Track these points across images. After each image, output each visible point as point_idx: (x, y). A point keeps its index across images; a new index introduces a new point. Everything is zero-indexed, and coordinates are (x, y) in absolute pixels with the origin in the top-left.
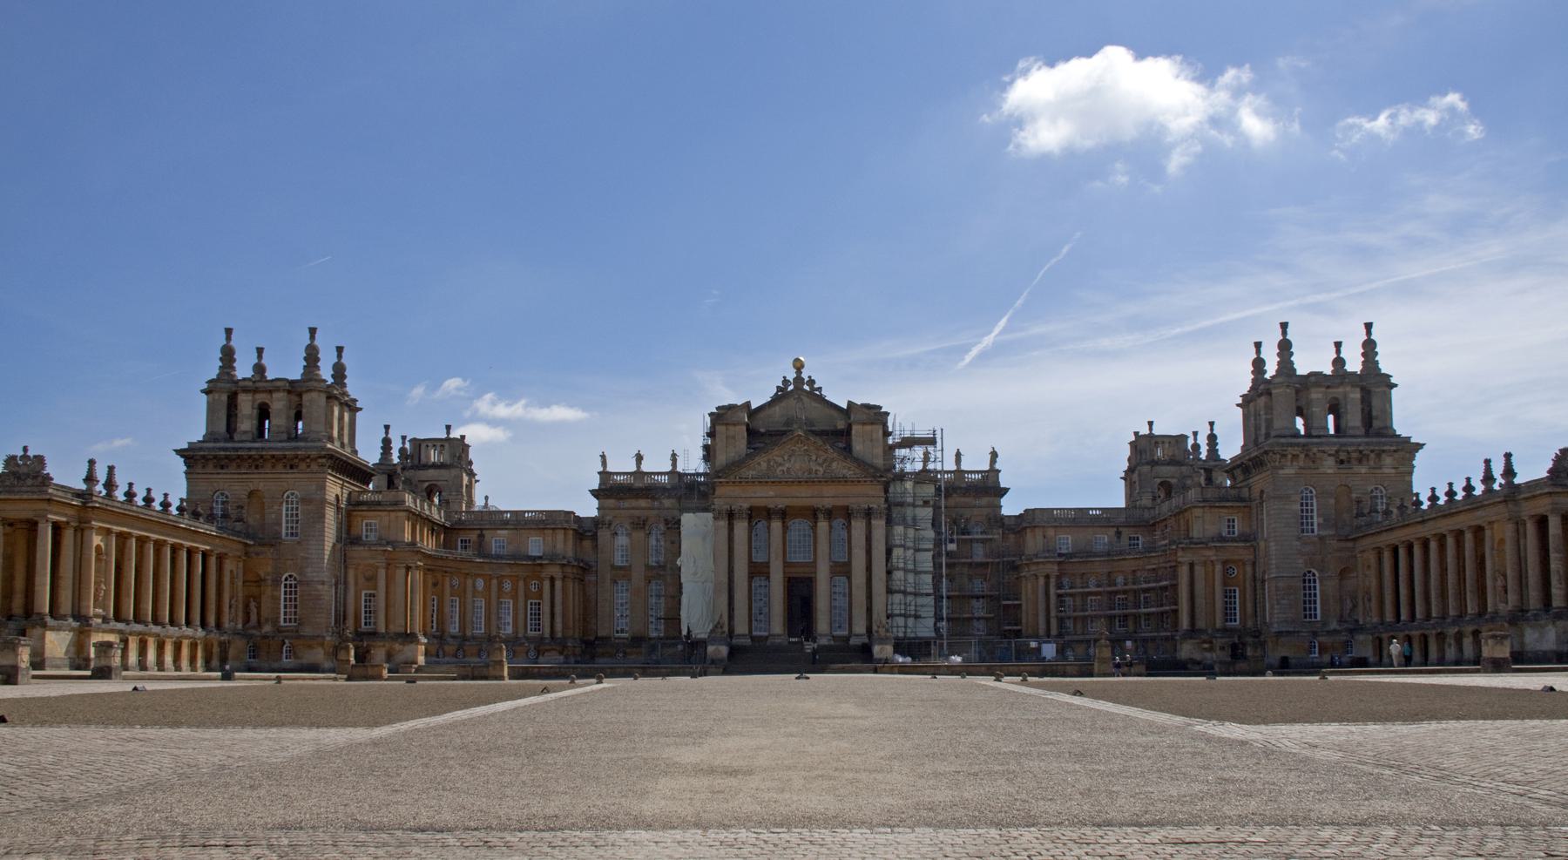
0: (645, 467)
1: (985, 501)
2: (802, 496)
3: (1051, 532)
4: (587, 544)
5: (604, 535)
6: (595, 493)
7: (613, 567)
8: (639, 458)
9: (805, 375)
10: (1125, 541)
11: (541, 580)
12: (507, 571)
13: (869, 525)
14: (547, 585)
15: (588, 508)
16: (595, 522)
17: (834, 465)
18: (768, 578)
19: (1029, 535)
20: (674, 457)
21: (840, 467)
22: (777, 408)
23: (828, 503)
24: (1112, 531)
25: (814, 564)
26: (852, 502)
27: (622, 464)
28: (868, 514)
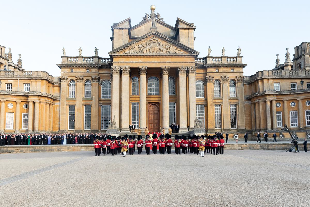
0: (83, 55)
1: (236, 70)
2: (154, 63)
3: (271, 81)
4: (56, 88)
5: (64, 85)
6: (61, 66)
7: (68, 99)
8: (80, 50)
9: (156, 12)
10: (305, 86)
11: (27, 103)
12: (10, 98)
13: (187, 76)
14: (31, 105)
15: (56, 73)
16: (60, 79)
17: (171, 48)
18: (138, 103)
19: (260, 82)
20: (96, 50)
21: (174, 50)
22: (143, 27)
23: (168, 66)
24: (299, 81)
25: (161, 97)
26: (179, 66)
27: (72, 52)
28: (187, 71)
